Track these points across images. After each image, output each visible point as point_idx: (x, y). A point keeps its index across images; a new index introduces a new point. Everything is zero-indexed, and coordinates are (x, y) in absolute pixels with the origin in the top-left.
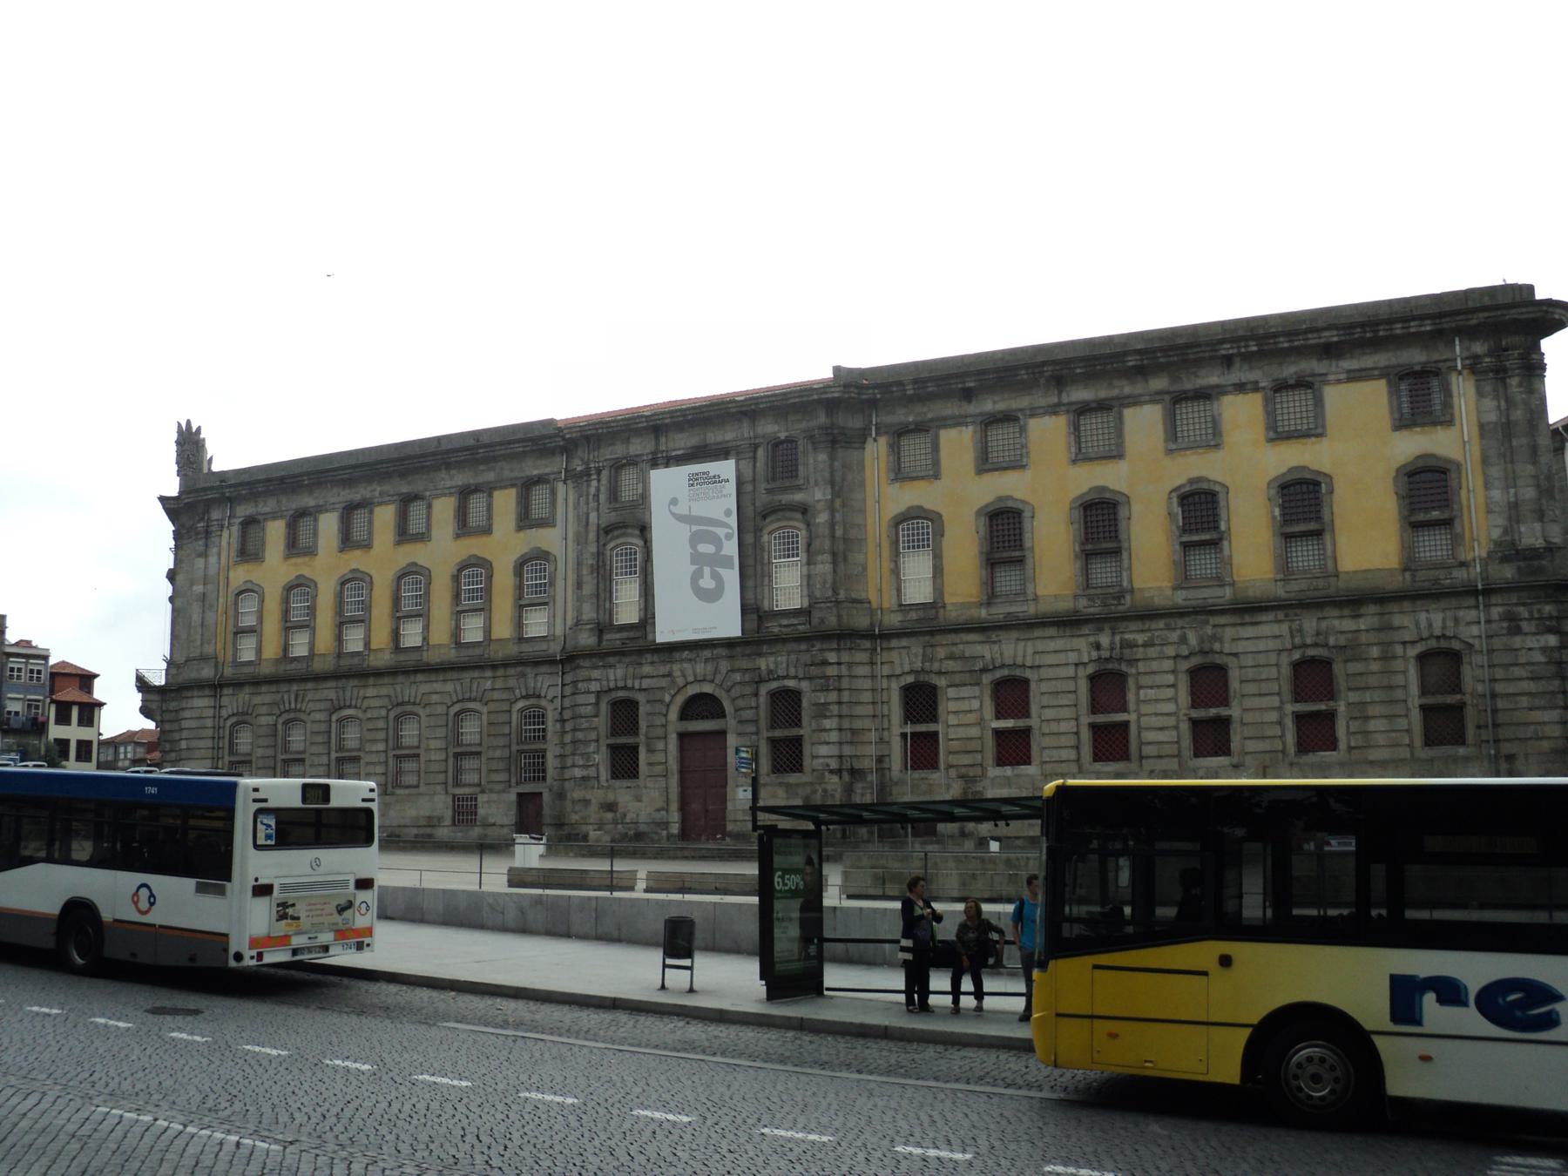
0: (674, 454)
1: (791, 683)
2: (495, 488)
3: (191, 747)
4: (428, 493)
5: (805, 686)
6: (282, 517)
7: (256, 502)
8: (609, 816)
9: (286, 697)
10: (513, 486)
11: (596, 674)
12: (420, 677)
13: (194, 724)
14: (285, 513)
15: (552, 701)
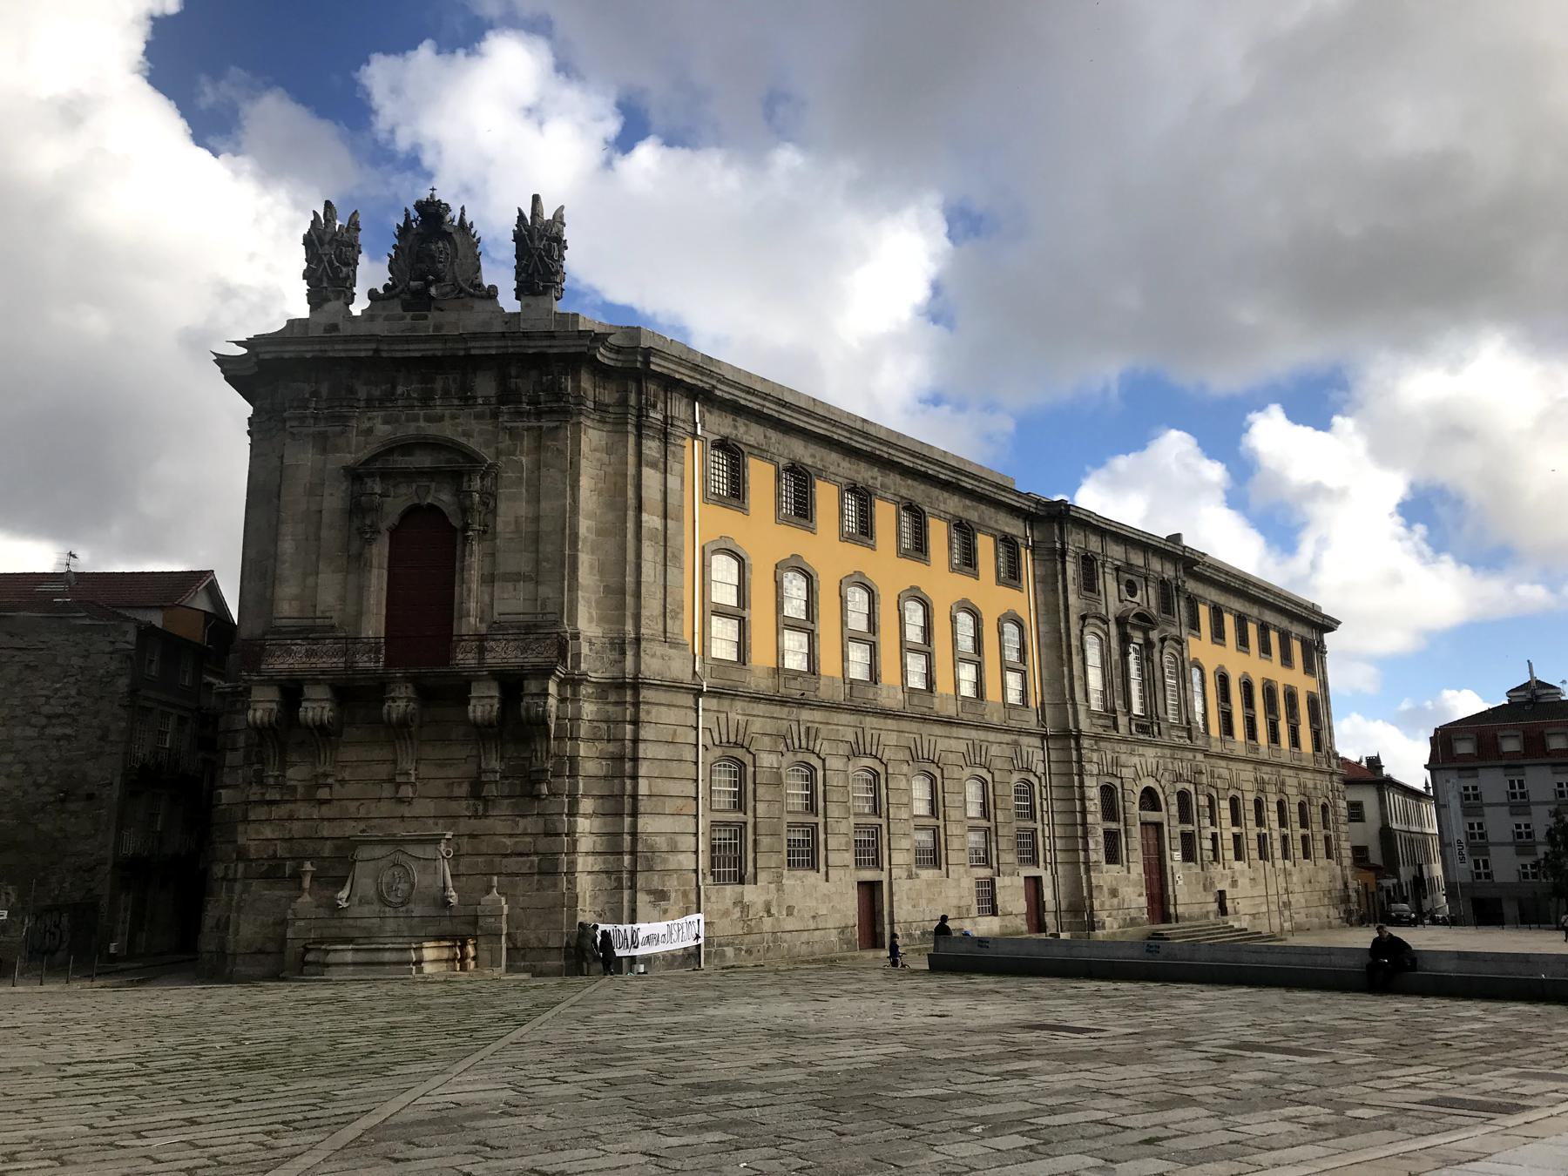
0: (1116, 562)
1: (1187, 786)
2: (979, 530)
3: (655, 791)
4: (926, 509)
5: (1191, 788)
6: (771, 460)
7: (734, 420)
8: (1115, 901)
9: (794, 728)
10: (992, 535)
11: (1095, 756)
12: (938, 730)
13: (662, 752)
14: (777, 458)
15: (1040, 779)
